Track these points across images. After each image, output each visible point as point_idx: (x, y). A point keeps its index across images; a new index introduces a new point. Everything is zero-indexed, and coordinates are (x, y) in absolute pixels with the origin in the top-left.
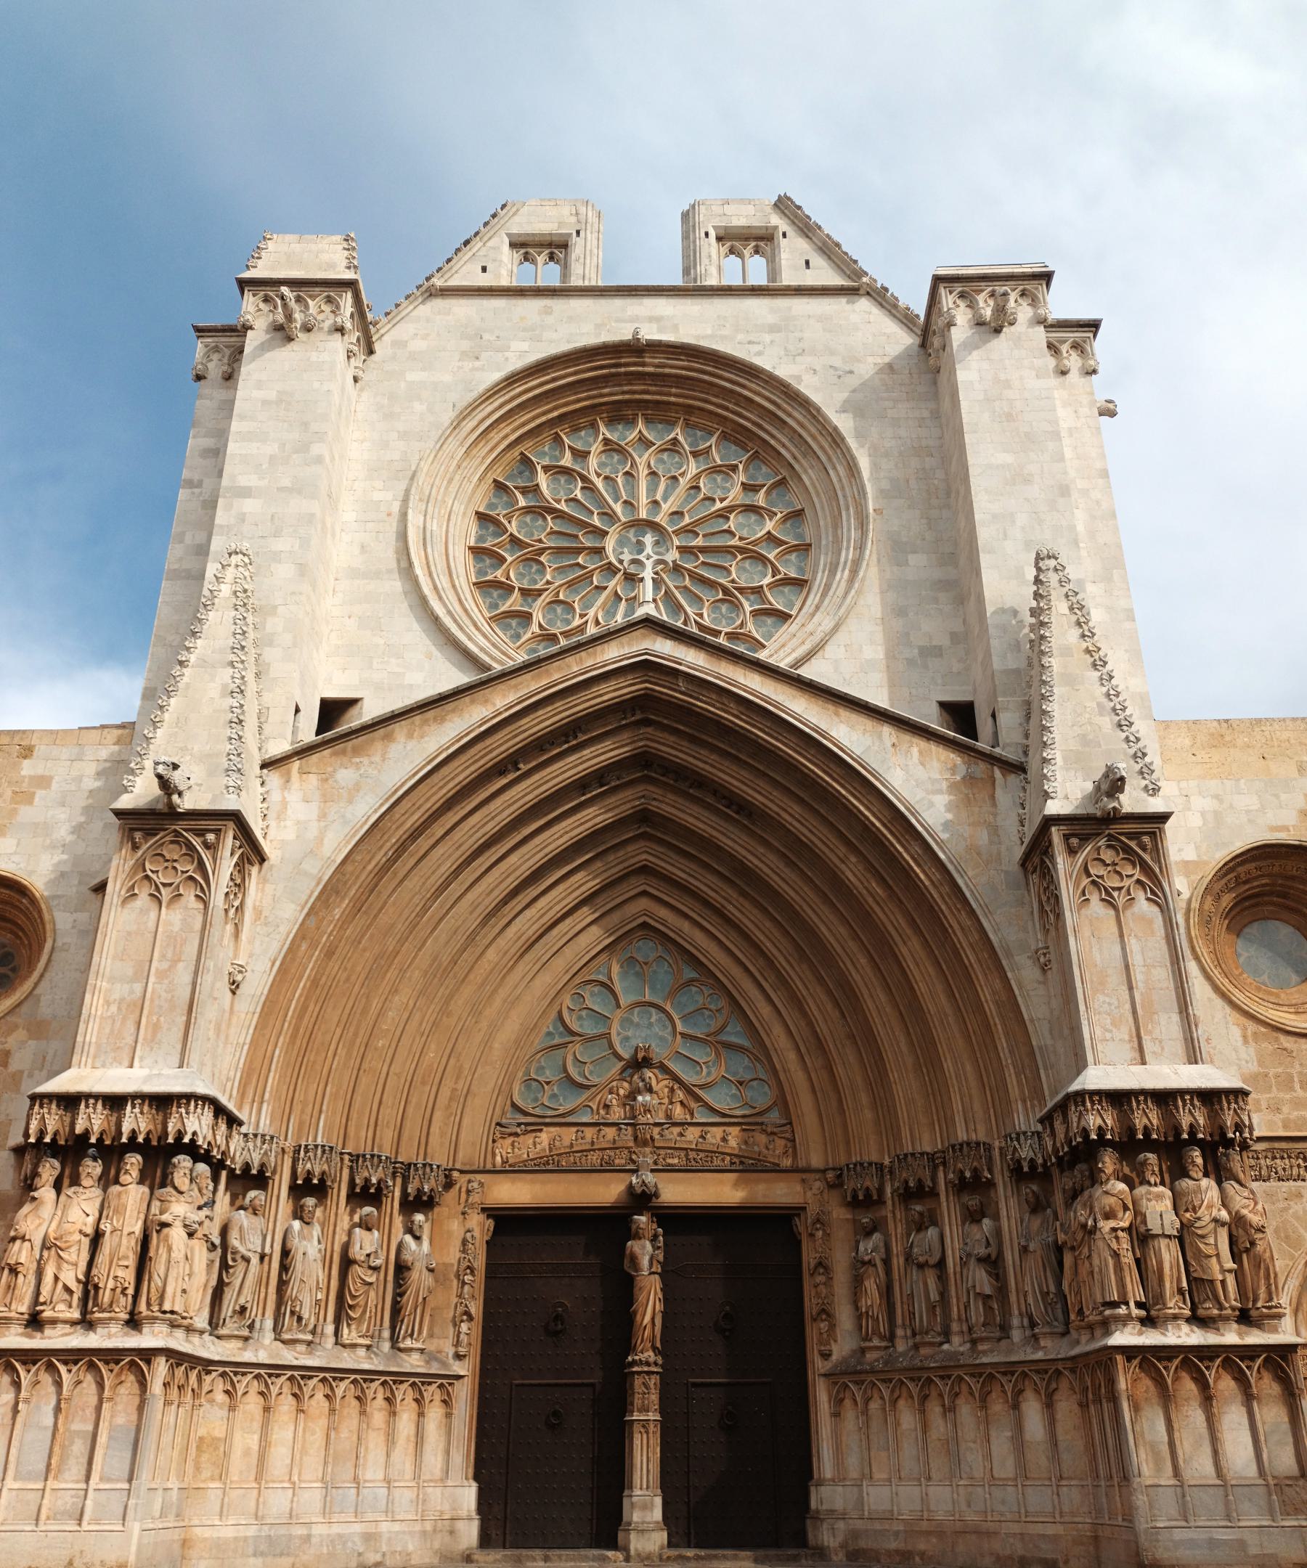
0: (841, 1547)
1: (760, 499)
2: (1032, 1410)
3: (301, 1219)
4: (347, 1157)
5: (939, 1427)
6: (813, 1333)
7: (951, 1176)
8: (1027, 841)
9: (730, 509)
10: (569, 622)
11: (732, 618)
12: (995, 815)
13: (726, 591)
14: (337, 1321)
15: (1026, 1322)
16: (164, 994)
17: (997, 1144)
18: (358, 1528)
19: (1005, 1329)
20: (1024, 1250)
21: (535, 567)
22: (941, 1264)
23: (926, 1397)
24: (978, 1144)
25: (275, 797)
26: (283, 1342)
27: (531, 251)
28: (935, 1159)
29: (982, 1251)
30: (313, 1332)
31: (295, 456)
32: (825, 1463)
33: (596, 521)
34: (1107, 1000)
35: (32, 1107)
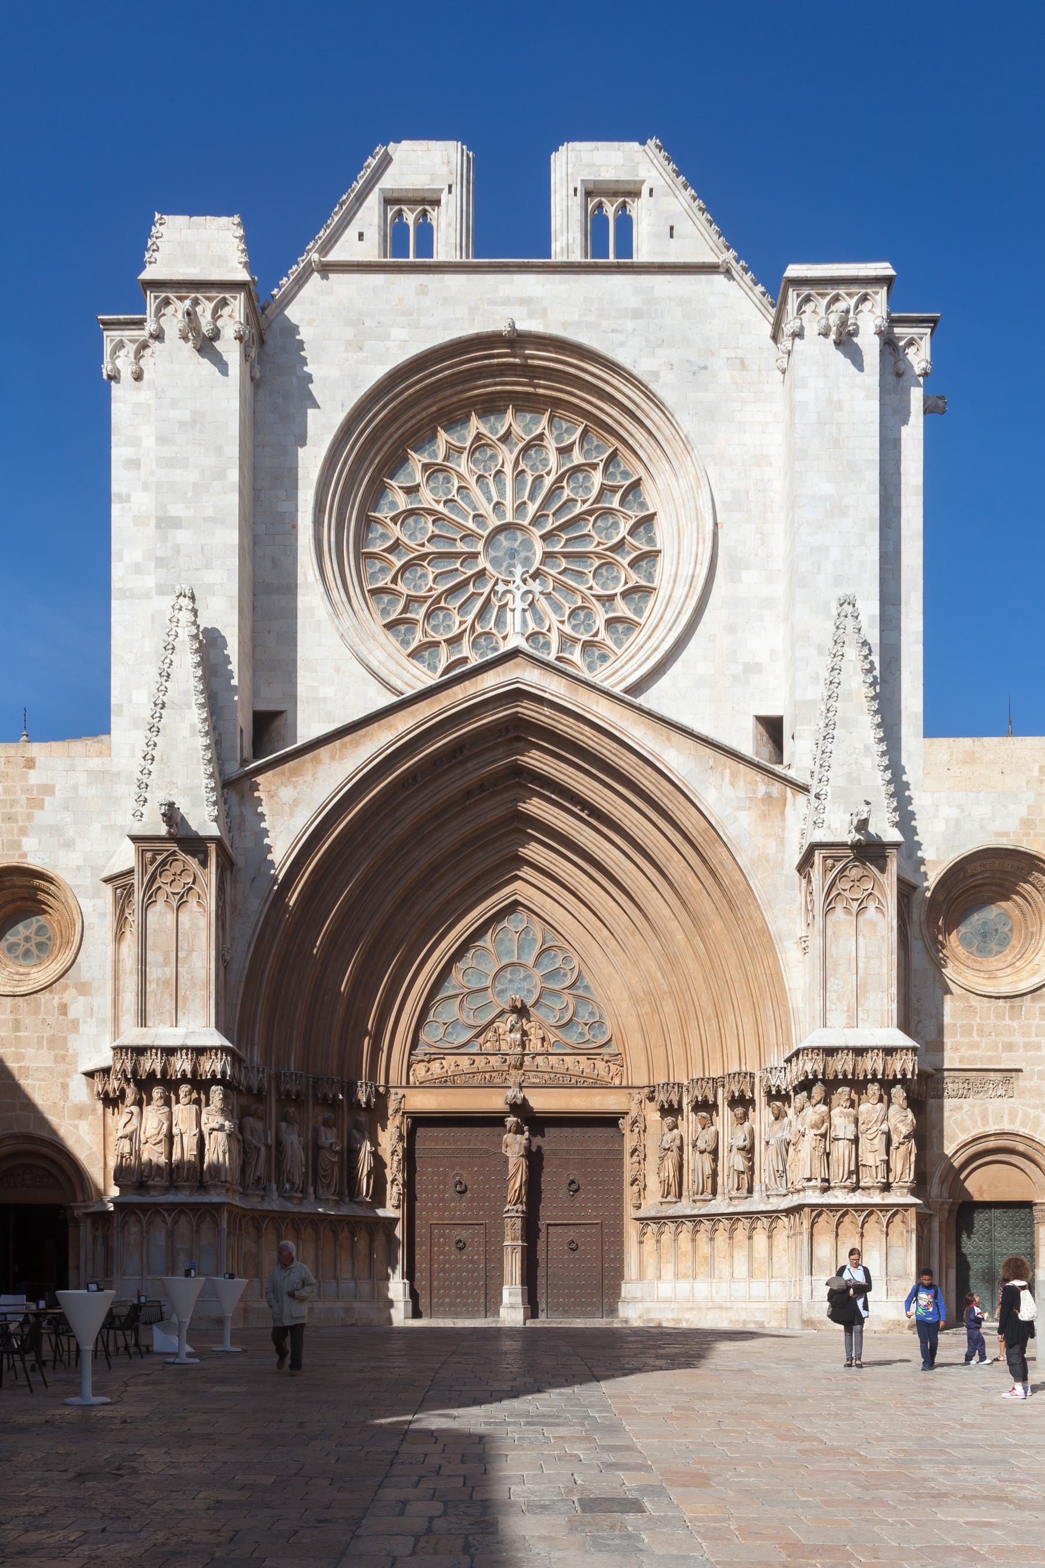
0: (640, 1317)
1: (615, 504)
2: (760, 1238)
3: (286, 1121)
4: (311, 1079)
5: (704, 1247)
6: (629, 1193)
7: (726, 1095)
8: (803, 851)
9: (589, 512)
10: (449, 627)
11: (589, 625)
12: (783, 829)
13: (584, 598)
14: (315, 1185)
15: (763, 1188)
16: (185, 975)
17: (758, 1074)
18: (340, 1304)
19: (750, 1190)
20: (768, 1143)
21: (419, 571)
22: (715, 1152)
23: (698, 1231)
24: (746, 1074)
25: (235, 811)
26: (285, 1198)
27: (404, 207)
28: (716, 1082)
29: (741, 1144)
30: (301, 1192)
31: (214, 483)
32: (631, 1268)
33: (470, 524)
34: (837, 981)
35: (115, 1055)
